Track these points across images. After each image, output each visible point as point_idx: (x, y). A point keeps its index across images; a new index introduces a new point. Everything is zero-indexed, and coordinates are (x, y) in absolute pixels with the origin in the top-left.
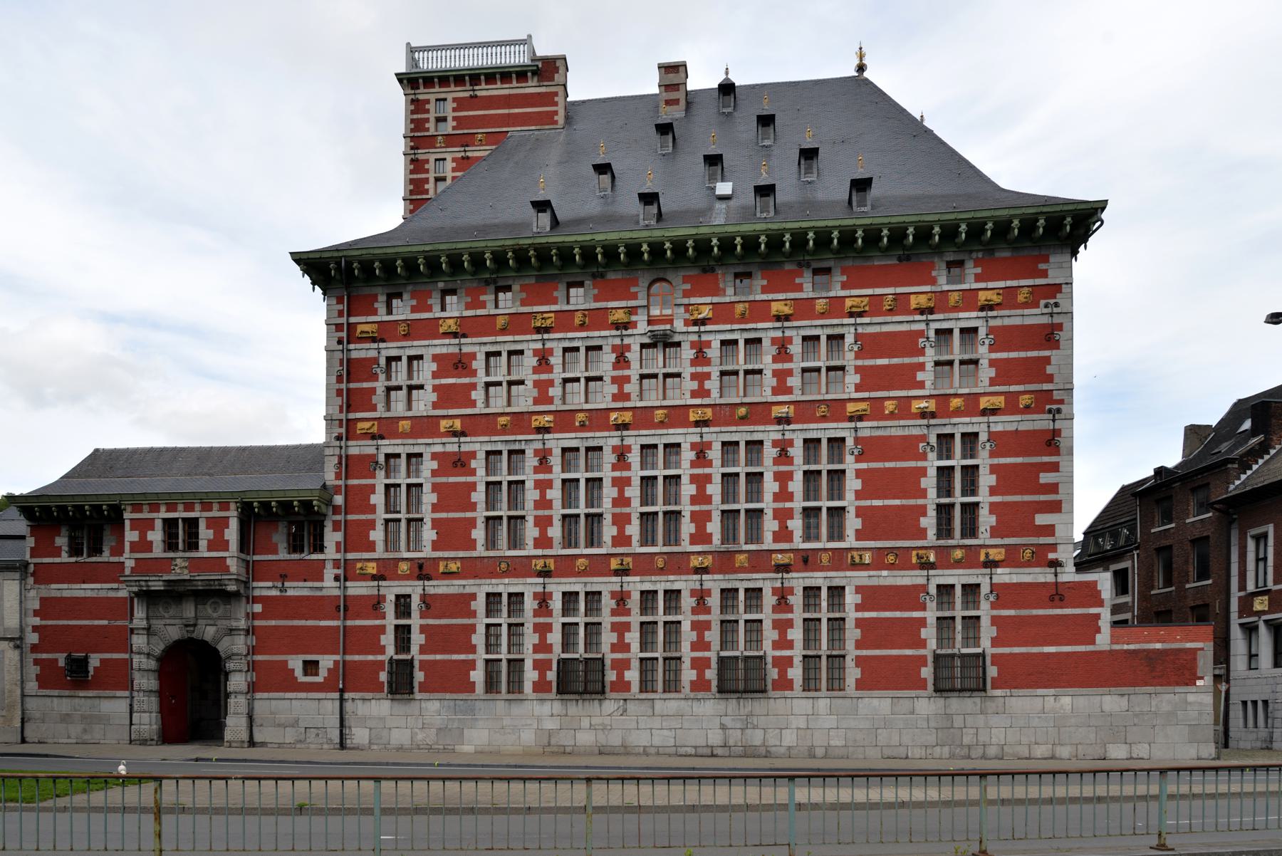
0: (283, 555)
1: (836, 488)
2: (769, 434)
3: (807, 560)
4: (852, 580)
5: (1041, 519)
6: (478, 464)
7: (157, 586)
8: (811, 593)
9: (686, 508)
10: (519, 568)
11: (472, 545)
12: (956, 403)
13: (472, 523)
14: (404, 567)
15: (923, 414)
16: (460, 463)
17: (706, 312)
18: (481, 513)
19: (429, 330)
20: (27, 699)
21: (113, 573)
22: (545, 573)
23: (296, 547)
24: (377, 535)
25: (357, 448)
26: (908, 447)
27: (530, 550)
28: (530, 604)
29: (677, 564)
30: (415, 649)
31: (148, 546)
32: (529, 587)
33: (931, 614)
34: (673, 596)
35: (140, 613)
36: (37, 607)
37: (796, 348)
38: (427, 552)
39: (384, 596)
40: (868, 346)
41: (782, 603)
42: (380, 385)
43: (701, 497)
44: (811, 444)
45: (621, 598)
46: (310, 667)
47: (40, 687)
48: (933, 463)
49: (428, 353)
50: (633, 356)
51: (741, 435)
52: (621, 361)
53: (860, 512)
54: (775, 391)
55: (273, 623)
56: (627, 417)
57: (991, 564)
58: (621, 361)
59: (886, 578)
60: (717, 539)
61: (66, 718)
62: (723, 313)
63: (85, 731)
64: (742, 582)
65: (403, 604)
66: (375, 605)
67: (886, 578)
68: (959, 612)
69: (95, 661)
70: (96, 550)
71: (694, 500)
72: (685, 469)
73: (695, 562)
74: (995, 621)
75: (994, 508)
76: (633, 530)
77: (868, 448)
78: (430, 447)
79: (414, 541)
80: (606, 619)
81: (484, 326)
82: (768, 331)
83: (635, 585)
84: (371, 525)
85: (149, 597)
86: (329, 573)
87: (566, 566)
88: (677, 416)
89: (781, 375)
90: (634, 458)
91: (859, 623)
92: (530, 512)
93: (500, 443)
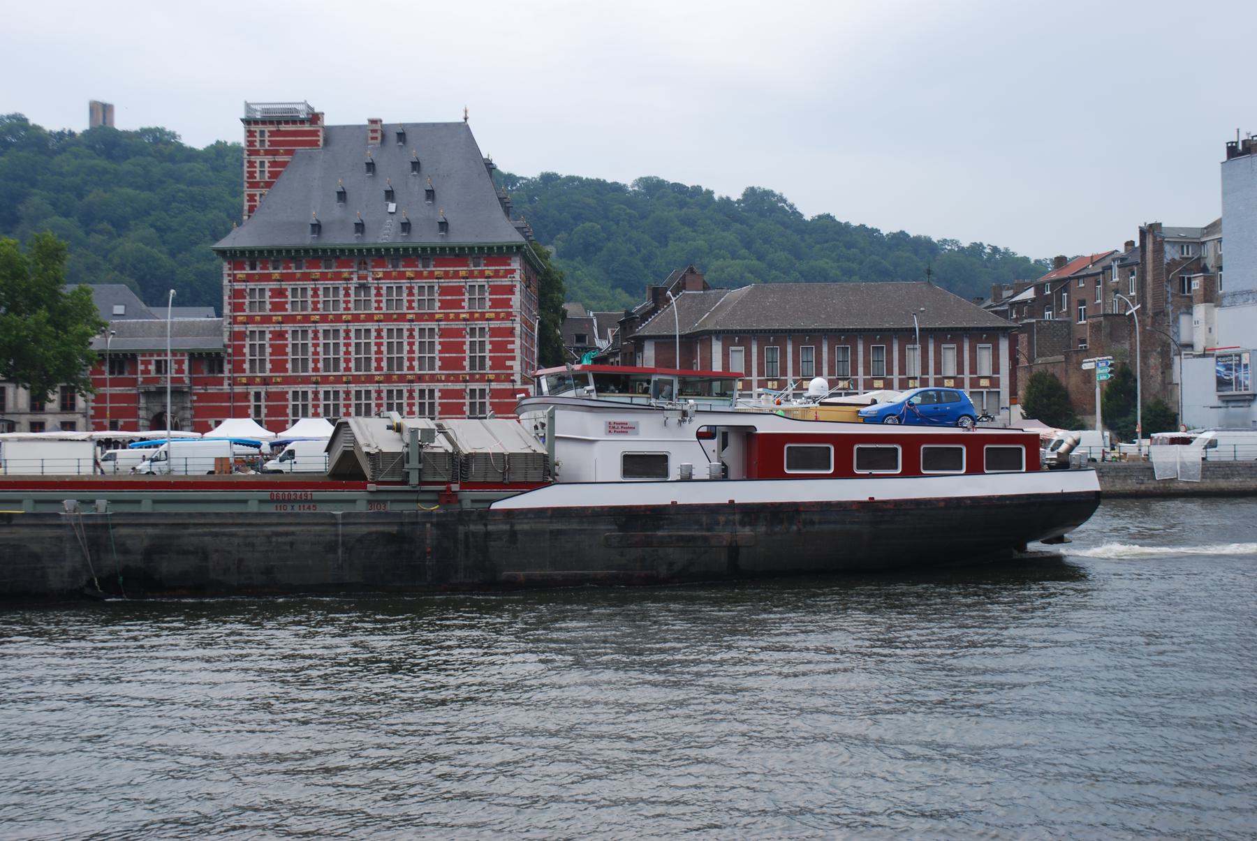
0: (206, 374)
1: (432, 350)
2: (405, 326)
3: (420, 378)
4: (437, 387)
5: (508, 363)
6: (289, 336)
7: (152, 389)
8: (422, 392)
9: (373, 356)
10: (306, 381)
11: (286, 371)
12: (477, 315)
13: (286, 361)
14: (258, 380)
15: (464, 320)
16: (280, 335)
17: (381, 275)
18: (290, 357)
19: (268, 278)
21: (133, 383)
22: (316, 383)
23: (211, 371)
24: (246, 366)
25: (237, 328)
26: (458, 333)
27: (310, 373)
28: (310, 396)
29: (370, 379)
30: (263, 415)
31: (148, 372)
32: (310, 389)
33: (467, 401)
34: (368, 393)
35: (142, 401)
37: (416, 291)
38: (268, 374)
40: (444, 291)
41: (411, 397)
42: (247, 301)
43: (379, 352)
44: (422, 330)
45: (347, 393)
48: (468, 339)
49: (267, 288)
50: (352, 292)
51: (394, 326)
52: (347, 294)
53: (441, 359)
54: (408, 308)
56: (349, 318)
57: (490, 381)
58: (347, 294)
59: (450, 386)
60: (385, 369)
62: (387, 276)
64: (395, 387)
65: (258, 395)
66: (245, 396)
67: (450, 386)
68: (478, 400)
69: (121, 422)
70: (121, 372)
71: (376, 353)
72: (373, 340)
73: (377, 378)
74: (491, 404)
75: (491, 358)
76: (352, 365)
77: (444, 333)
78: (268, 328)
79: (262, 370)
80: (342, 402)
81: (290, 277)
82: (405, 283)
83: (353, 388)
84: (244, 361)
85: (147, 394)
86: (226, 382)
87: (325, 380)
88: (370, 318)
89: (410, 302)
90: (352, 334)
91: (440, 404)
92: (310, 357)
93: (297, 327)
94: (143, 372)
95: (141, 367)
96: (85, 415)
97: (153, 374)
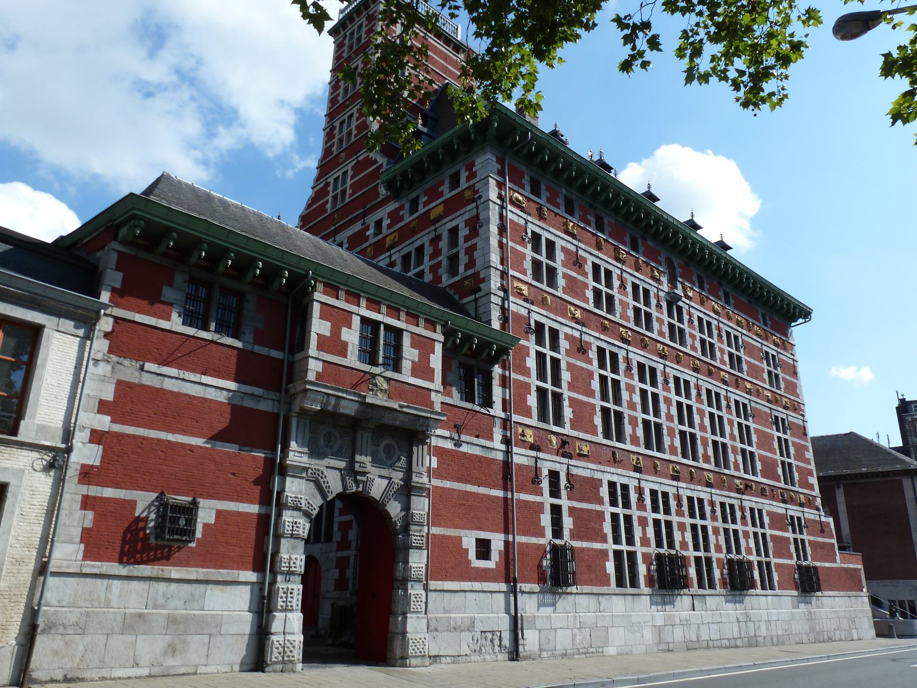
20: (51, 581)
36: (108, 394)
38: (567, 430)
39: (541, 469)
47: (88, 555)
55: (448, 484)
61: (134, 624)
63: (172, 650)
94: (323, 343)
95: (319, 327)
96: (57, 461)
97: (352, 360)
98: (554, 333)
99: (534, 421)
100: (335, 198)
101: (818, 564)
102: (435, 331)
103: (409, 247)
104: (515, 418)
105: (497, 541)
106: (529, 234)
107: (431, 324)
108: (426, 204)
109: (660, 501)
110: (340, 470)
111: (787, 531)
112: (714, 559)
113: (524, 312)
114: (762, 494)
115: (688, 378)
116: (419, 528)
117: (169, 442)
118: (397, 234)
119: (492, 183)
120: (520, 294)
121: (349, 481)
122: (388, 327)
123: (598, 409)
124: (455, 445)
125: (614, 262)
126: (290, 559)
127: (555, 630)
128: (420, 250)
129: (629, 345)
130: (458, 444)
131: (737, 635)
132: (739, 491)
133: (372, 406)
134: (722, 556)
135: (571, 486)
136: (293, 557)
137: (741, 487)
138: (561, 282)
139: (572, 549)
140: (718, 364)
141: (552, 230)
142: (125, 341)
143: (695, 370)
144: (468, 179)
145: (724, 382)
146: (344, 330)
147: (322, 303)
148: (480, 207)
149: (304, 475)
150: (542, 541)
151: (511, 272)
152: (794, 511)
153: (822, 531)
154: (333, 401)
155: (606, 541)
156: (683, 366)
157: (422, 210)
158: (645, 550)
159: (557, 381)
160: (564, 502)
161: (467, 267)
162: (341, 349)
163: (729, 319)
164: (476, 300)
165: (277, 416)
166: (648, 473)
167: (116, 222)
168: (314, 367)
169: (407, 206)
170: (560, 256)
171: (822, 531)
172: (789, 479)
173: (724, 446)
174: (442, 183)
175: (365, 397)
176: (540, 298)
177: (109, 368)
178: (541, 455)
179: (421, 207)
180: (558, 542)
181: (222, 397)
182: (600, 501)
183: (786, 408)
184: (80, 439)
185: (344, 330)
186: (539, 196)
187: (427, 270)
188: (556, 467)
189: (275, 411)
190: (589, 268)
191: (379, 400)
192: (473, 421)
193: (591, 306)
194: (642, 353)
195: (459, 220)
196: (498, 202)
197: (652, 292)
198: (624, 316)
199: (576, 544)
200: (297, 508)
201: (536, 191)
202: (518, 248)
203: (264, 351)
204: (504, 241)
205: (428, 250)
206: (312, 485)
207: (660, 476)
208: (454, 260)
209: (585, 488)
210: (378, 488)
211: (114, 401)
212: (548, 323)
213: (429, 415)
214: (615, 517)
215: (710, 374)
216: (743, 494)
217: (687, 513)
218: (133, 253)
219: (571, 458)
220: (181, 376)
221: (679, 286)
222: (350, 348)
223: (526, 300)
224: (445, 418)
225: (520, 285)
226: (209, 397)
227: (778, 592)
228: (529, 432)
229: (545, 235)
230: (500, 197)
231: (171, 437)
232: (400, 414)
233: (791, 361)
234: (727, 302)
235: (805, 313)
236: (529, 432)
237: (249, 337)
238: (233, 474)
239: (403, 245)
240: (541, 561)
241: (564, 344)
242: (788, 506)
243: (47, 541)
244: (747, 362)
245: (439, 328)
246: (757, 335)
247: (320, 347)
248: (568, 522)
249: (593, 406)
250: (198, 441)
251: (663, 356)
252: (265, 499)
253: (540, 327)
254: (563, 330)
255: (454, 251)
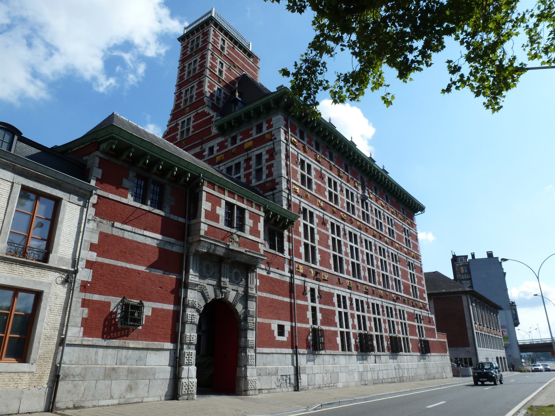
20: (67, 349)
36: (95, 241)
38: (318, 266)
46: (281, 329)
47: (85, 334)
61: (110, 374)
63: (130, 388)
95: (206, 206)
96: (69, 278)
97: (221, 224)
98: (311, 214)
99: (303, 261)
100: (182, 133)
101: (428, 339)
102: (260, 210)
103: (231, 163)
104: (295, 259)
105: (287, 326)
106: (299, 160)
107: (258, 207)
108: (241, 140)
109: (360, 305)
110: (213, 286)
111: (415, 322)
112: (384, 336)
113: (297, 202)
114: (404, 302)
115: (371, 240)
116: (252, 318)
117: (127, 268)
118: (223, 155)
119: (282, 131)
120: (296, 192)
121: (218, 292)
122: (238, 207)
123: (332, 255)
124: (267, 273)
125: (337, 177)
126: (191, 335)
127: (315, 374)
128: (238, 165)
129: (345, 222)
130: (269, 272)
131: (395, 376)
132: (394, 301)
133: (232, 250)
134: (387, 334)
135: (320, 297)
136: (192, 334)
137: (395, 298)
138: (314, 187)
139: (322, 330)
140: (383, 233)
141: (310, 158)
142: (105, 210)
143: (374, 236)
144: (268, 128)
145: (386, 243)
146: (218, 207)
147: (207, 192)
148: (276, 144)
149: (197, 288)
150: (308, 326)
151: (292, 180)
152: (418, 311)
153: (430, 322)
154: (213, 247)
155: (336, 326)
156: (369, 234)
157: (239, 143)
158: (354, 331)
159: (313, 240)
160: (318, 305)
161: (267, 176)
162: (216, 218)
163: (388, 210)
164: (273, 194)
165: (182, 255)
166: (354, 290)
167: (98, 140)
168: (204, 228)
169: (229, 140)
170: (313, 173)
171: (430, 322)
172: (415, 295)
173: (387, 276)
174: (252, 129)
175: (229, 245)
176: (305, 195)
177: (96, 225)
178: (307, 279)
179: (238, 141)
180: (316, 327)
181: (154, 243)
182: (333, 305)
183: (413, 257)
184: (82, 264)
185: (218, 207)
186: (303, 140)
187: (242, 176)
188: (314, 286)
189: (181, 252)
190: (326, 180)
191: (234, 247)
192: (276, 260)
193: (327, 200)
194: (350, 226)
195: (263, 150)
196: (285, 141)
197: (355, 194)
198: (342, 207)
199: (324, 328)
200: (193, 307)
201: (302, 137)
202: (295, 167)
203: (175, 218)
204: (288, 163)
205: (243, 165)
206: (200, 294)
207: (359, 292)
208: (259, 172)
209: (326, 298)
210: (231, 296)
211: (98, 244)
212: (309, 209)
213: (258, 256)
214: (340, 313)
215: (380, 238)
216: (396, 302)
217: (372, 312)
218: (108, 159)
219: (320, 281)
220: (134, 231)
221: (367, 192)
222: (220, 218)
223: (299, 196)
224: (266, 258)
225: (296, 187)
226: (147, 243)
227: (412, 353)
228: (301, 267)
229: (307, 161)
230: (286, 139)
231: (129, 266)
232: (244, 255)
233: (415, 233)
234: (387, 201)
235: (421, 209)
236: (301, 267)
237: (168, 209)
238: (160, 287)
239: (227, 162)
240: (308, 337)
241: (316, 220)
242: (415, 309)
243: (64, 325)
244: (396, 233)
245: (262, 209)
246: (400, 219)
247: (206, 217)
248: (319, 316)
249: (329, 254)
250: (142, 268)
251: (360, 228)
252: (177, 302)
253: (305, 210)
254: (316, 213)
255: (260, 167)
